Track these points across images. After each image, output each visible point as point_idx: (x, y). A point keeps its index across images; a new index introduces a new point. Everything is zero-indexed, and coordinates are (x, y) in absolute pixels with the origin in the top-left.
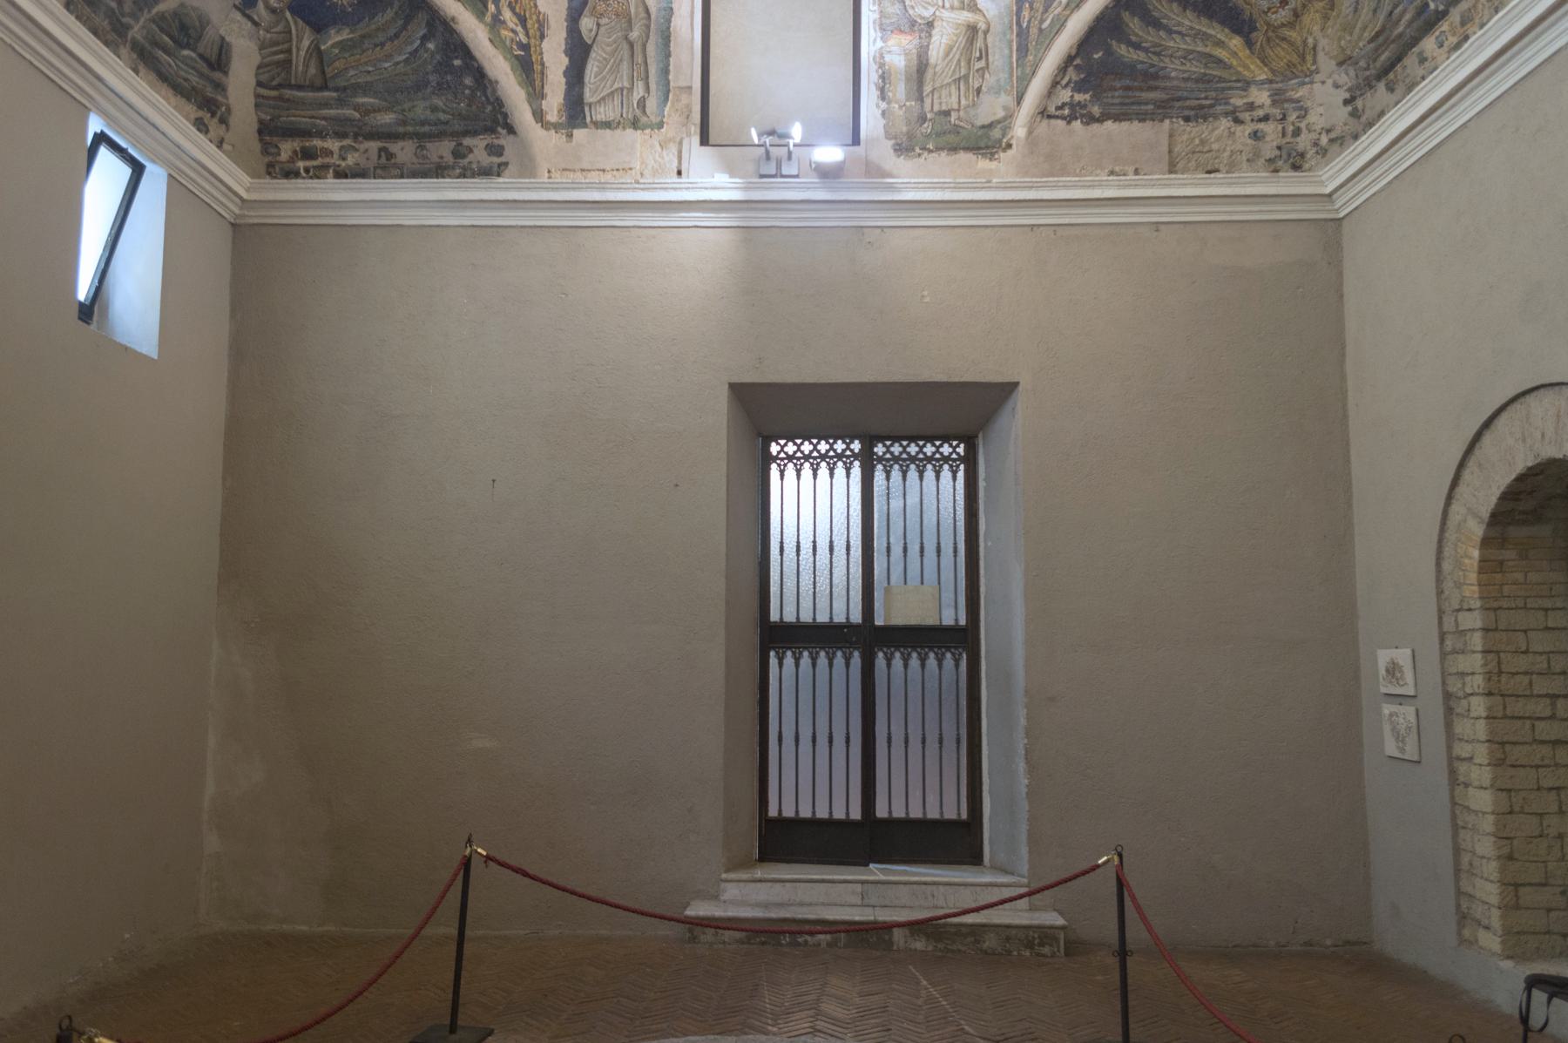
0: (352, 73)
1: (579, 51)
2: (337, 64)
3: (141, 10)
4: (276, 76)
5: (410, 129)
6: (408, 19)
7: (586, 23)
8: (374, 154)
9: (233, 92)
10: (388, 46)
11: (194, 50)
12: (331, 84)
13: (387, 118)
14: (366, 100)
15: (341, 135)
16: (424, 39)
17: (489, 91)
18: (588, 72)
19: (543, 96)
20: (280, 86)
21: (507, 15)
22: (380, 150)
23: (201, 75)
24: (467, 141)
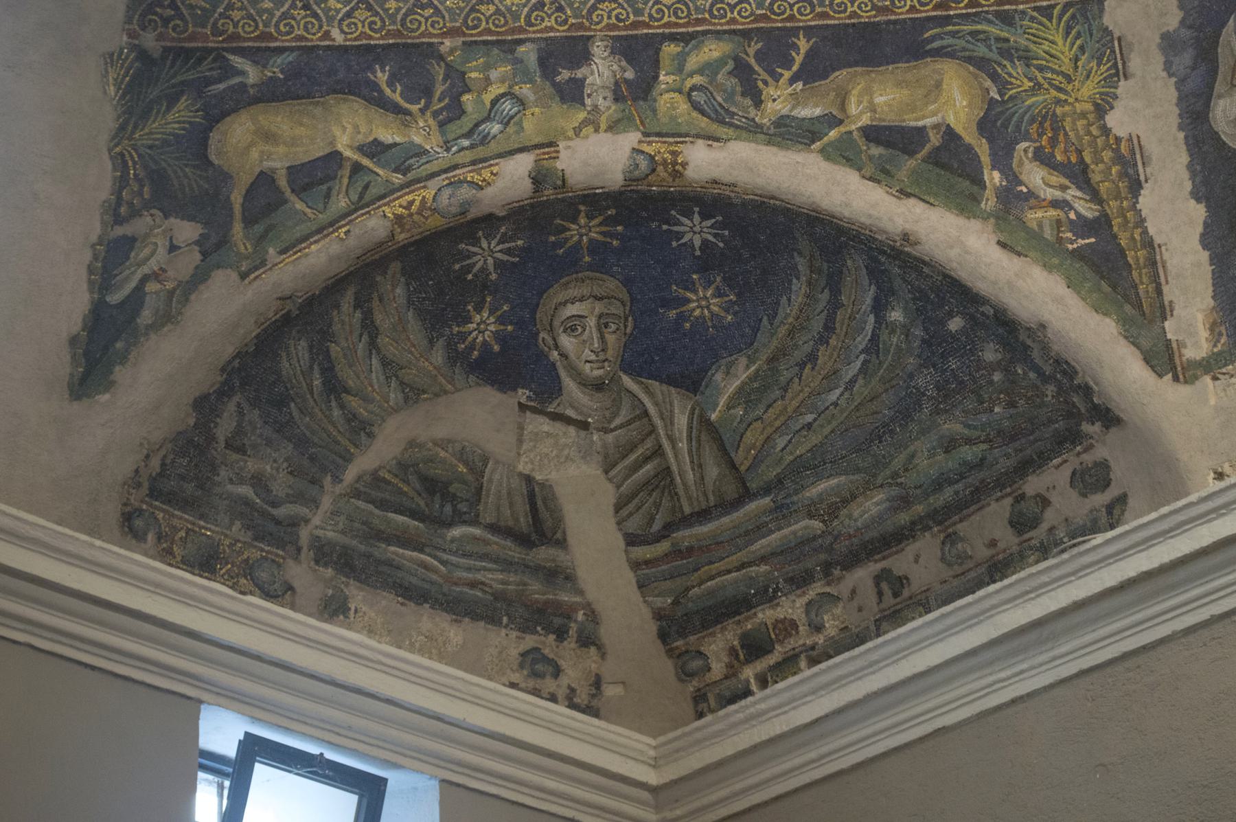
0: (781, 442)
2: (749, 437)
4: (657, 517)
5: (920, 509)
6: (834, 284)
9: (586, 575)
10: (823, 354)
11: (475, 522)
12: (753, 485)
13: (872, 506)
14: (822, 486)
15: (800, 581)
16: (879, 308)
17: (1036, 354)
19: (1163, 311)
20: (668, 528)
21: (1035, 177)
22: (878, 579)
23: (507, 565)
24: (1033, 485)
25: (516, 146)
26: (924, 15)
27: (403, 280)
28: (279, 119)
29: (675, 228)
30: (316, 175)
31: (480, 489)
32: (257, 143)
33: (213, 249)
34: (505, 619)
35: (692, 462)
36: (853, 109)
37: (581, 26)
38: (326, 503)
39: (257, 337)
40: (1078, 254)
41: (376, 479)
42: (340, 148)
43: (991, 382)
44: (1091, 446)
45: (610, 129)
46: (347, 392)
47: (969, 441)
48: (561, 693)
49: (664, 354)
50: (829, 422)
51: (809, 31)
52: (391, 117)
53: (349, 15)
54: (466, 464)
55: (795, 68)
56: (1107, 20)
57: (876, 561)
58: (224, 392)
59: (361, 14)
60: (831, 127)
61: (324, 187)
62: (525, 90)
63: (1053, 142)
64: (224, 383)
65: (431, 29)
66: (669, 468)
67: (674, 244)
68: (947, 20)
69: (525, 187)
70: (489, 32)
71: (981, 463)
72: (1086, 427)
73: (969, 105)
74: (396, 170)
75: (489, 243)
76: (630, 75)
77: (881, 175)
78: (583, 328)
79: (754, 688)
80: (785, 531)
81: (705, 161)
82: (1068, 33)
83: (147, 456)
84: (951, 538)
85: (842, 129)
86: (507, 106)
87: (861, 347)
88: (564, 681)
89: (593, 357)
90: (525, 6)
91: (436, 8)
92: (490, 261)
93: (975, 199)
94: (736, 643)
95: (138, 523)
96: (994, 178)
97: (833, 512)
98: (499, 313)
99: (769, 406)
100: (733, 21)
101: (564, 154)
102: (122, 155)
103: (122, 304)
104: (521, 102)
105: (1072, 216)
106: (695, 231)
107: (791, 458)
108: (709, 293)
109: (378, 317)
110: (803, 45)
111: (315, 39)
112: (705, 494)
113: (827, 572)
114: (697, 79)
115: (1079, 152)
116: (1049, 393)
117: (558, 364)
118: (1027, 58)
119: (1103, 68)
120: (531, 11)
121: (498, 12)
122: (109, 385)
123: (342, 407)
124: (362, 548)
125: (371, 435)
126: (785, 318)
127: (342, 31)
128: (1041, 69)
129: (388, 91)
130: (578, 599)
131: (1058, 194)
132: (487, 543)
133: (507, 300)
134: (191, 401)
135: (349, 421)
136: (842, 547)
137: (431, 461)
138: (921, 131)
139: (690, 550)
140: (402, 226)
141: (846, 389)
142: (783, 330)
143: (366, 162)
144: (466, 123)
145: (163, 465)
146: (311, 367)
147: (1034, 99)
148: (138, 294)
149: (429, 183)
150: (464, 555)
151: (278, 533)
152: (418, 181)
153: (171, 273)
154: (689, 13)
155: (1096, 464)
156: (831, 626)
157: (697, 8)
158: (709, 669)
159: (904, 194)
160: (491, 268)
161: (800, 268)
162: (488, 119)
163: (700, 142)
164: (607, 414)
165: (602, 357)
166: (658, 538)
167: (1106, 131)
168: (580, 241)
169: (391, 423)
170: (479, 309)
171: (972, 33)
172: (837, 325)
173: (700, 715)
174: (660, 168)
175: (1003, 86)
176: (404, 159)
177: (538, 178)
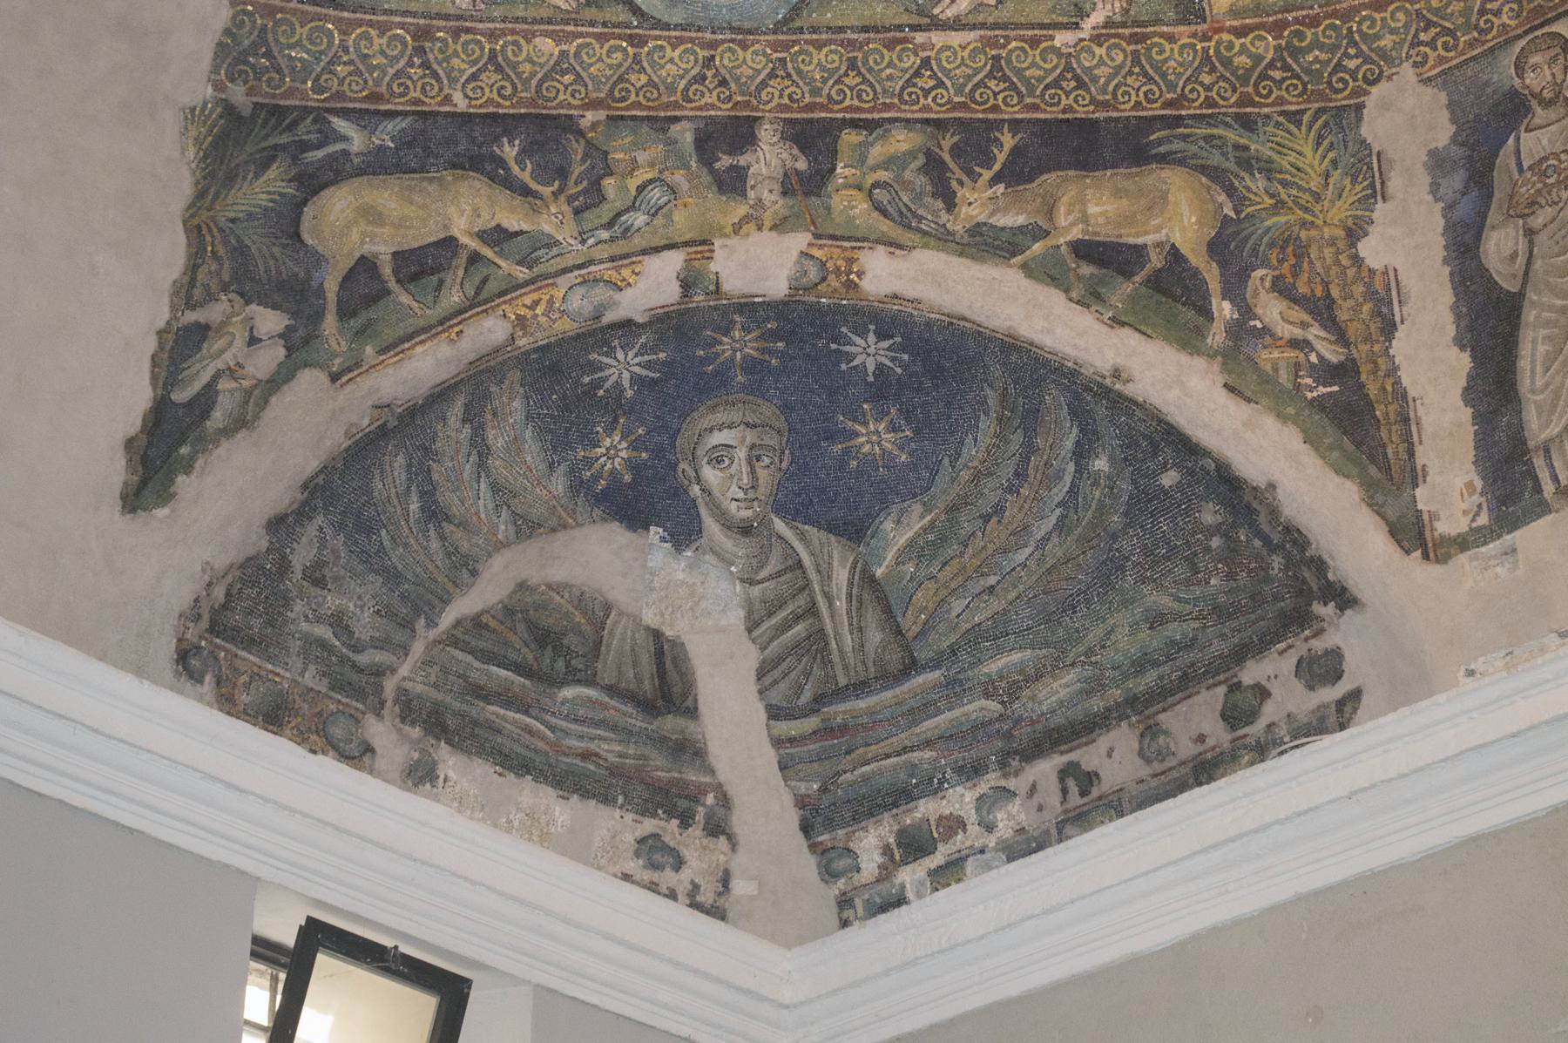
1: (1490, 322)
3: (407, 625)
4: (808, 688)
5: (1116, 694)
7: (1500, 246)
8: (1050, 786)
11: (591, 682)
12: (922, 655)
14: (1003, 661)
16: (1081, 454)
17: (1262, 519)
18: (1524, 364)
19: (1415, 477)
20: (819, 700)
21: (1272, 311)
22: (1064, 773)
24: (1252, 673)
25: (664, 242)
26: (1150, 113)
27: (522, 391)
28: (386, 196)
29: (847, 348)
30: (423, 264)
31: (598, 644)
32: (354, 222)
33: (300, 347)
34: (621, 799)
35: (851, 625)
36: (1062, 220)
37: (747, 104)
38: (418, 649)
39: (346, 450)
40: (1319, 405)
41: (477, 623)
42: (456, 232)
43: (1208, 549)
44: (1318, 633)
45: (774, 227)
46: (448, 519)
47: (1179, 617)
48: (682, 891)
49: (824, 496)
50: (1015, 587)
51: (1015, 125)
52: (518, 200)
53: (474, 77)
54: (584, 613)
55: (997, 167)
56: (1365, 131)
57: (1062, 753)
58: (303, 512)
59: (489, 77)
60: (1035, 239)
61: (435, 279)
62: (679, 178)
63: (1296, 270)
64: (305, 503)
65: (570, 100)
67: (844, 367)
68: (1178, 121)
69: (669, 293)
70: (638, 105)
71: (1190, 644)
72: (1318, 608)
73: (1199, 222)
74: (519, 263)
76: (802, 165)
77: (1092, 297)
78: (729, 459)
79: (910, 895)
80: (957, 712)
81: (884, 274)
82: (1319, 144)
83: (210, 584)
84: (1151, 731)
85: (1050, 242)
86: (656, 195)
87: (1057, 500)
88: (686, 874)
89: (741, 495)
90: (682, 77)
91: (578, 74)
92: (626, 375)
93: (1200, 333)
94: (891, 840)
95: (195, 663)
96: (1224, 310)
97: (1013, 692)
99: (944, 564)
100: (926, 109)
101: (719, 254)
102: (199, 227)
103: (189, 404)
104: (673, 190)
105: (1313, 358)
106: (868, 353)
107: (968, 626)
109: (491, 434)
110: (1008, 140)
111: (432, 105)
112: (864, 663)
113: (1003, 765)
114: (883, 175)
115: (1326, 284)
116: (1276, 565)
118: (1269, 170)
119: (1358, 188)
120: (690, 84)
121: (651, 82)
122: (166, 496)
123: (442, 538)
124: (457, 705)
125: (474, 573)
127: (466, 96)
128: (1285, 184)
129: (516, 170)
130: (708, 779)
131: (1298, 332)
132: (605, 707)
133: (642, 422)
135: (449, 555)
136: (1023, 733)
138: (1139, 251)
139: (844, 729)
140: (524, 328)
141: (1037, 548)
142: (965, 475)
143: (487, 252)
144: (606, 212)
145: (228, 595)
146: (408, 489)
147: (1275, 219)
148: (208, 396)
149: (559, 280)
150: (576, 721)
151: (358, 684)
152: (545, 276)
153: (250, 370)
154: (876, 98)
155: (1327, 652)
156: (1004, 829)
157: (885, 91)
158: (858, 870)
159: (1117, 322)
160: (626, 384)
162: (632, 207)
163: (881, 249)
164: (754, 562)
165: (751, 495)
166: (805, 713)
167: (1357, 260)
169: (498, 562)
170: (609, 432)
171: (1208, 139)
173: (845, 924)
174: (832, 277)
175: (1239, 202)
176: (531, 249)
177: (687, 284)
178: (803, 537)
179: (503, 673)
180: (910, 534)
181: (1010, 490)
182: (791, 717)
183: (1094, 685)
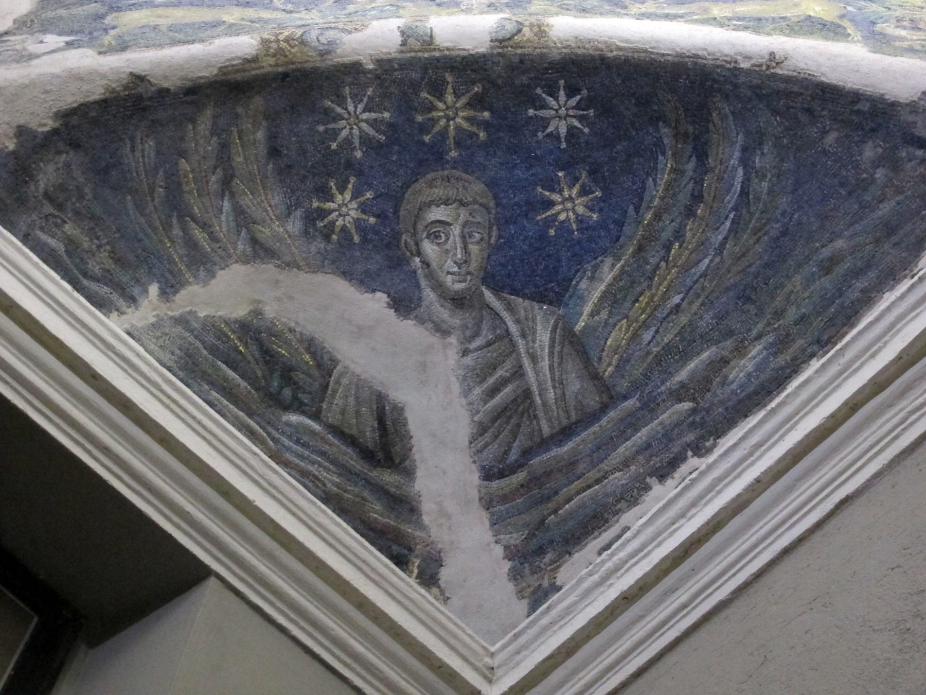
0: (647, 336)
11: (316, 416)
20: (527, 453)
23: (346, 471)
27: (264, 123)
35: (553, 380)
46: (194, 219)
49: (530, 268)
66: (529, 389)
67: (540, 135)
75: (356, 107)
92: (356, 131)
98: (362, 199)
108: (575, 191)
117: (419, 271)
123: (184, 230)
126: (651, 201)
132: (327, 442)
133: (370, 186)
134: (14, 124)
137: (275, 336)
139: (548, 474)
146: (156, 170)
159: (769, 34)
160: (356, 142)
161: (666, 141)
166: (513, 469)
168: (447, 126)
170: (342, 189)
172: (706, 195)
178: (510, 308)
179: (231, 374)
180: (603, 287)
181: (688, 217)
182: (501, 475)
183: (783, 343)
